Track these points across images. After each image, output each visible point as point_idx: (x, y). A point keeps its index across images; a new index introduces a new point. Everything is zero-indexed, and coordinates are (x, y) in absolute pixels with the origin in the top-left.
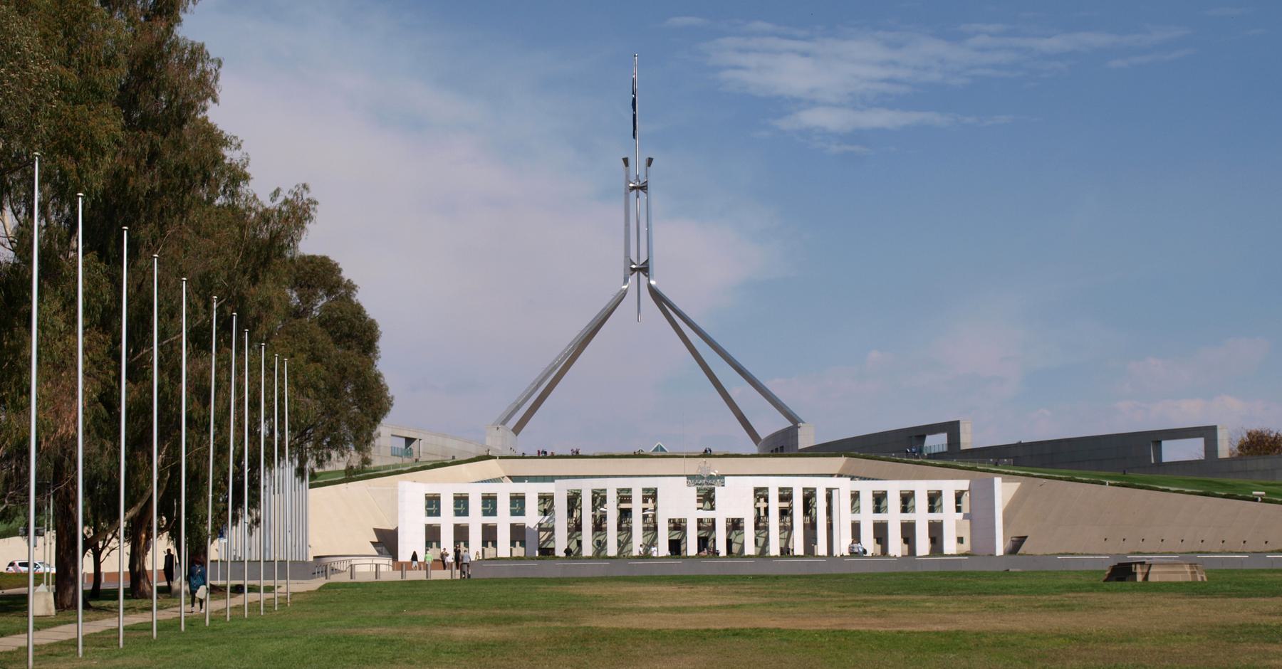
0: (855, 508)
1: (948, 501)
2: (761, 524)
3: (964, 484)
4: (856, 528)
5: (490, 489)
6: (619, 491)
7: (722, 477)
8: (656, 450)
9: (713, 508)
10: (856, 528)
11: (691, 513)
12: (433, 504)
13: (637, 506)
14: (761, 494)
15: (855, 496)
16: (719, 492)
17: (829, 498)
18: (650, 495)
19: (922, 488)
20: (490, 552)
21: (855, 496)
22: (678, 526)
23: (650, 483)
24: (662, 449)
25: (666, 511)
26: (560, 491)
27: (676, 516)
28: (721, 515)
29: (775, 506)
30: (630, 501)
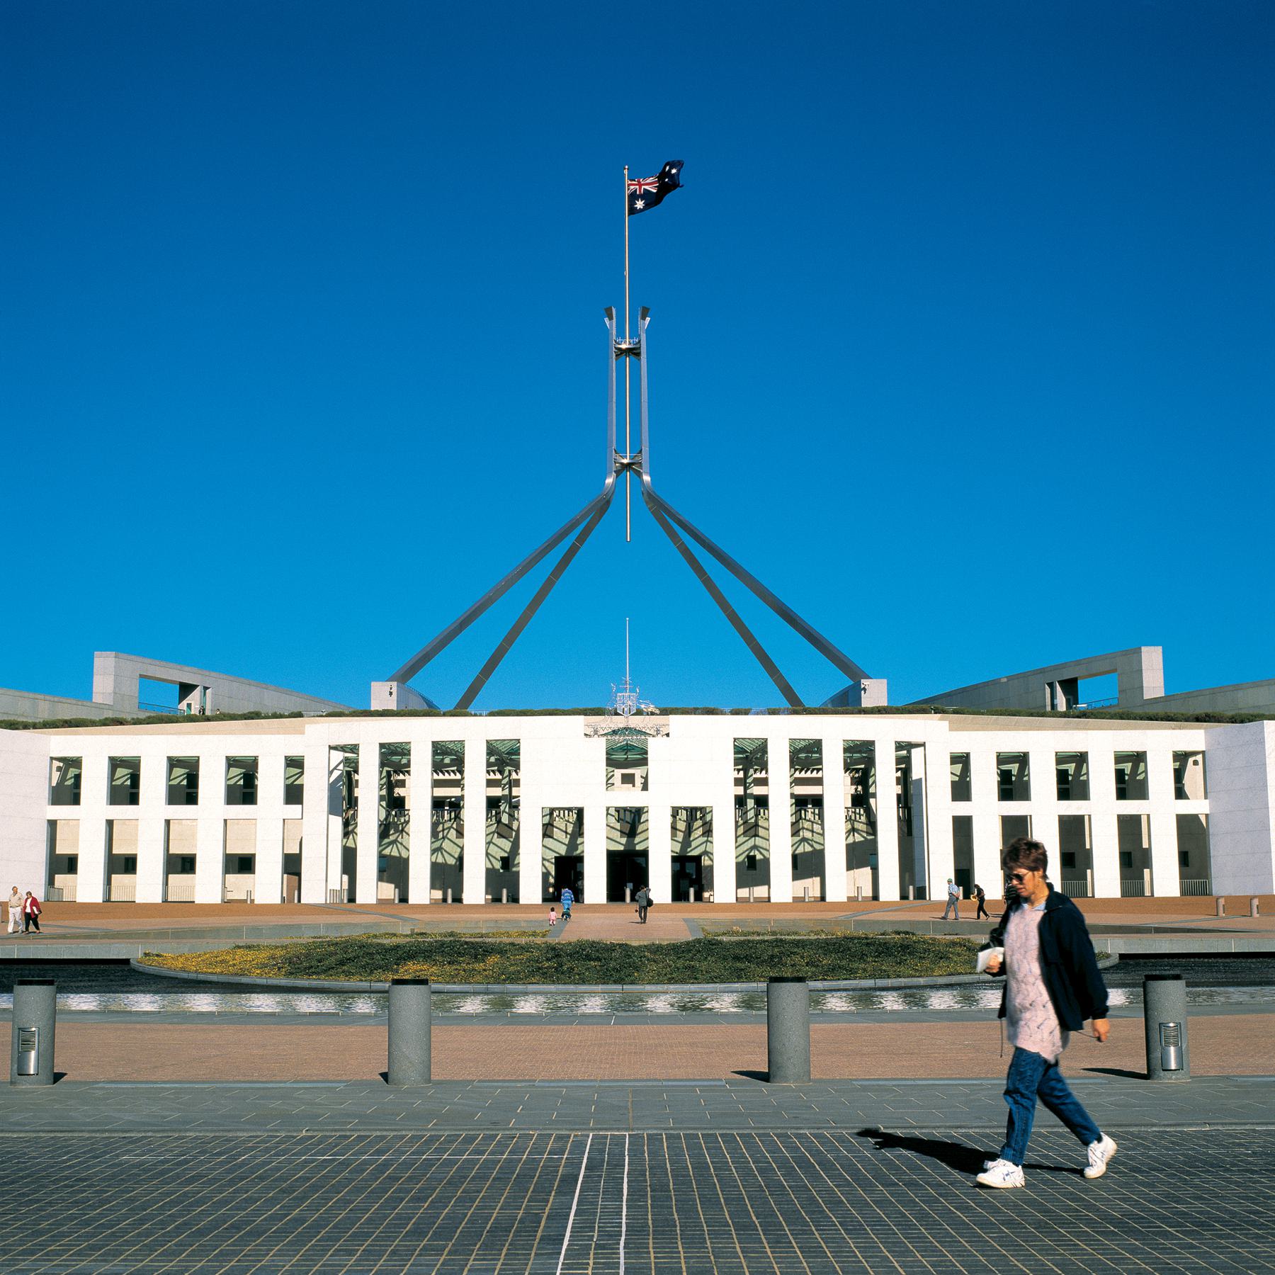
0: (961, 790)
1: (1159, 775)
3: (1193, 738)
4: (963, 828)
6: (440, 749)
9: (645, 787)
10: (963, 828)
11: (599, 799)
14: (750, 758)
16: (655, 747)
17: (904, 766)
18: (504, 759)
19: (1102, 745)
20: (240, 884)
21: (962, 760)
29: (779, 783)
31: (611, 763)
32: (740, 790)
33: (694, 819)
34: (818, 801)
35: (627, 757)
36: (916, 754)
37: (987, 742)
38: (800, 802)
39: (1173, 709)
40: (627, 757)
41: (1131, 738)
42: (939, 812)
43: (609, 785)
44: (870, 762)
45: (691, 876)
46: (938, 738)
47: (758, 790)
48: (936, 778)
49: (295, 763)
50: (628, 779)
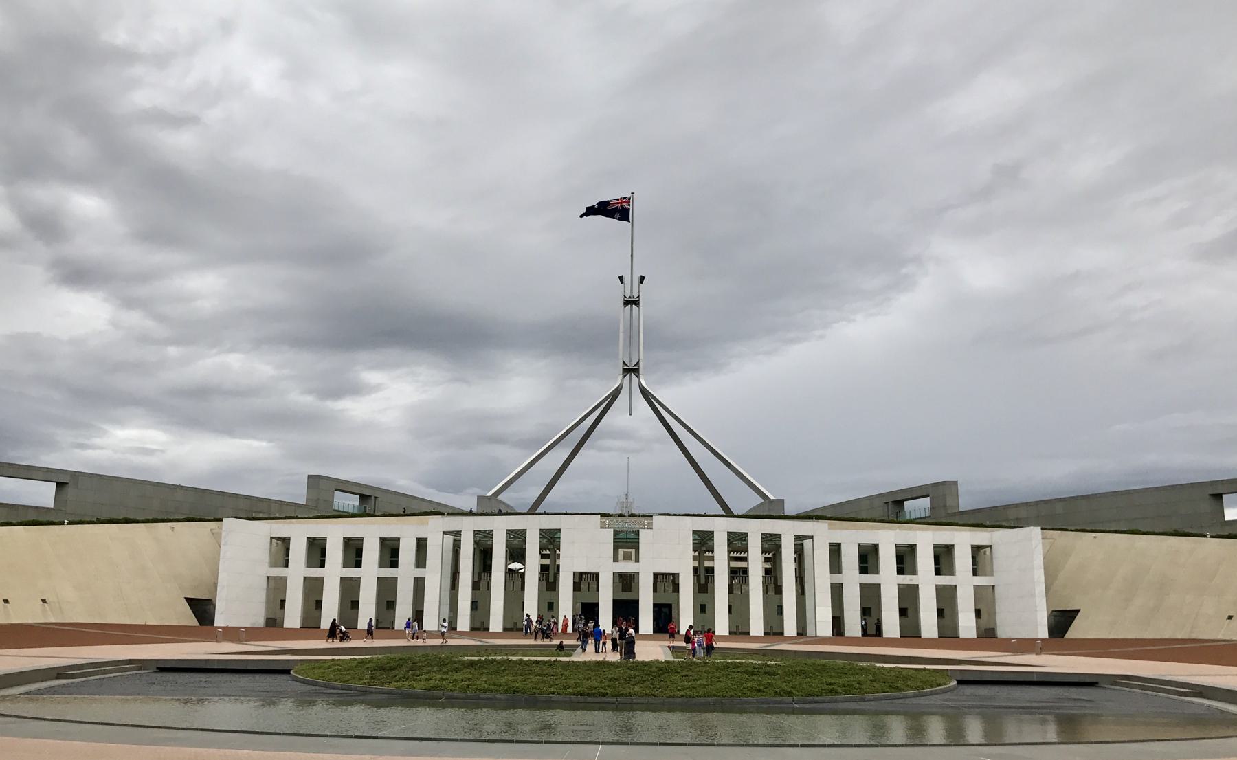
0: (836, 567)
4: (837, 591)
9: (637, 560)
10: (837, 591)
14: (703, 542)
15: (835, 550)
18: (551, 540)
21: (835, 550)
25: (570, 563)
31: (616, 548)
32: (697, 564)
33: (666, 582)
34: (745, 571)
35: (626, 543)
36: (807, 544)
37: (851, 537)
38: (733, 572)
39: (929, 521)
40: (626, 543)
41: (944, 535)
42: (821, 578)
43: (616, 559)
44: (778, 548)
45: (665, 619)
46: (822, 534)
47: (707, 564)
49: (421, 545)
50: (627, 557)
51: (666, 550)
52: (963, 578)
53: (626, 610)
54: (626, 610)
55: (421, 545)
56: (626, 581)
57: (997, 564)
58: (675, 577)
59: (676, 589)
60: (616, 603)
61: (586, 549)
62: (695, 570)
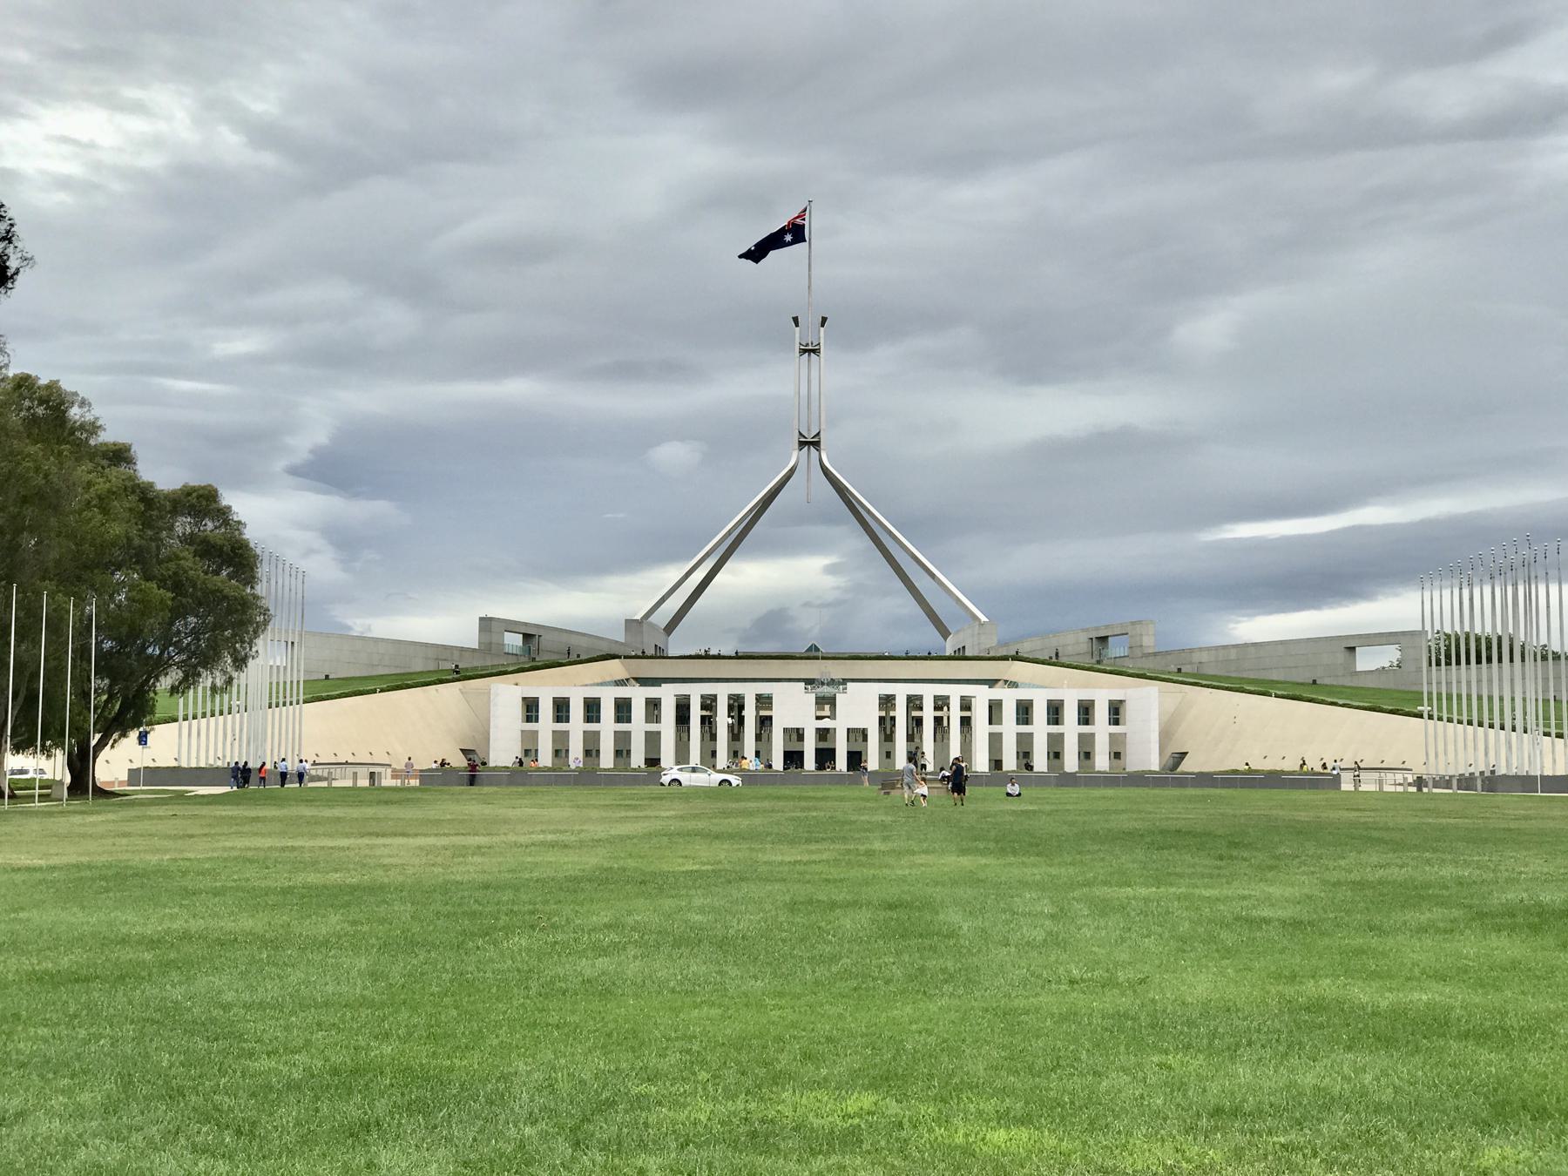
2: (887, 735)
4: (995, 741)
5: (623, 692)
7: (845, 681)
8: (810, 649)
10: (995, 741)
12: (531, 708)
13: (928, 715)
14: (887, 702)
18: (764, 701)
22: (799, 734)
23: (764, 688)
24: (817, 649)
25: (782, 719)
26: (668, 695)
27: (793, 724)
28: (840, 726)
29: (900, 713)
30: (921, 709)
48: (980, 714)
51: (858, 708)
52: (1101, 727)
53: (825, 756)
54: (825, 756)
55: (653, 706)
56: (823, 734)
57: (1129, 713)
58: (864, 734)
59: (865, 738)
60: (818, 751)
61: (794, 708)
62: (882, 719)
